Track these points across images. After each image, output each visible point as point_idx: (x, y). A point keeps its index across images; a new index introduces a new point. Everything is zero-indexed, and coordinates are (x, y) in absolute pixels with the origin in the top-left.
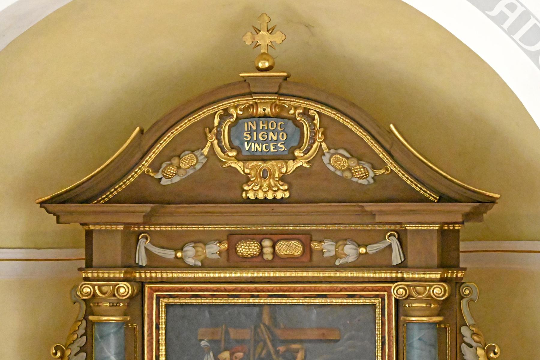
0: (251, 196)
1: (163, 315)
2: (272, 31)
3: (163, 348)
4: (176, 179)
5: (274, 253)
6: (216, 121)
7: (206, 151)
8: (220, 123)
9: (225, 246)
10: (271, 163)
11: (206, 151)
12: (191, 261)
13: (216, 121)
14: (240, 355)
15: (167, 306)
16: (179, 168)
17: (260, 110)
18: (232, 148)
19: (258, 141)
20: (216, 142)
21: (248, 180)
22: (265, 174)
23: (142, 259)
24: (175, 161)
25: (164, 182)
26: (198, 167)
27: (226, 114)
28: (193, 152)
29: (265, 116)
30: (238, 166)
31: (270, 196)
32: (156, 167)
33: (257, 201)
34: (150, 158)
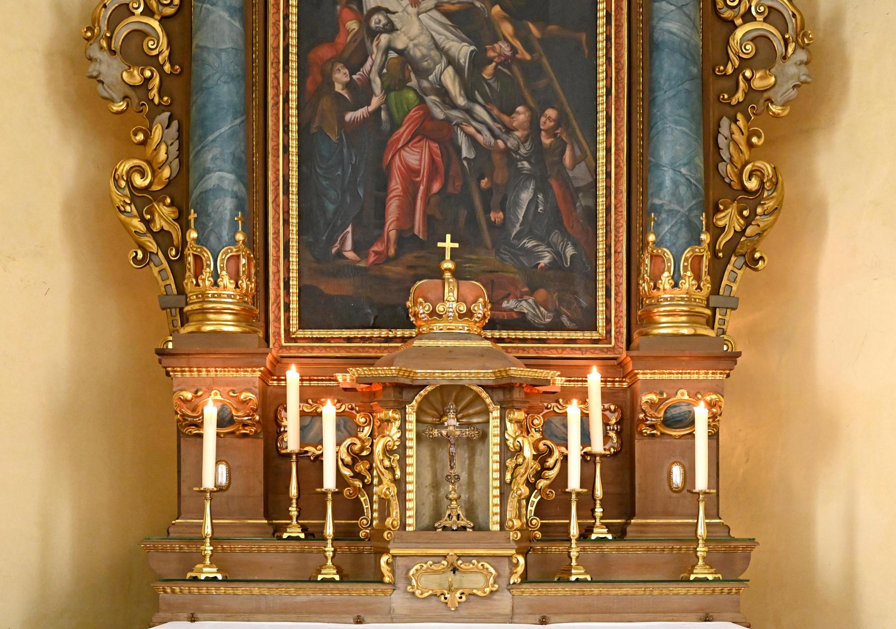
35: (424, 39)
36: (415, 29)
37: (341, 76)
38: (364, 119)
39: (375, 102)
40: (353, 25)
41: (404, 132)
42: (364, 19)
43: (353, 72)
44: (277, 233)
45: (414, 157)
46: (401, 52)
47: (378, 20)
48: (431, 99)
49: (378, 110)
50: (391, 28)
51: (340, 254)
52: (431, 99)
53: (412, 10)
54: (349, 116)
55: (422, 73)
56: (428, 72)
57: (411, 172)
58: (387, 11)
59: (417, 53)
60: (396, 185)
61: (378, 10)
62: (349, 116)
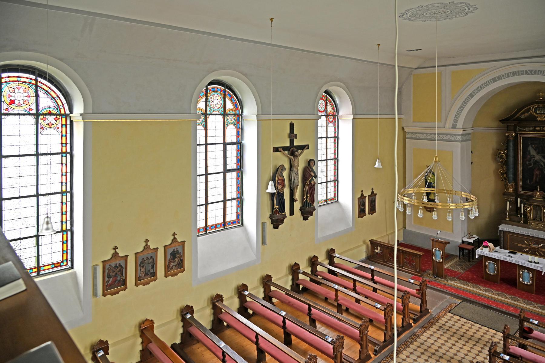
0: (538, 120)
1: (521, 139)
2: (542, 93)
3: (521, 144)
4: (524, 117)
5: (543, 129)
6: (532, 108)
7: (530, 113)
8: (532, 108)
9: (533, 128)
10: (542, 115)
11: (530, 113)
12: (527, 130)
13: (532, 108)
14: (536, 146)
15: (522, 137)
16: (524, 115)
17: (540, 106)
18: (535, 112)
19: (540, 111)
20: (531, 111)
21: (538, 117)
22: (541, 116)
23: (517, 129)
24: (524, 114)
25: (522, 117)
26: (528, 115)
27: (533, 107)
28: (527, 113)
29: (541, 107)
30: (536, 115)
31: (542, 120)
32: (520, 115)
33: (539, 121)
34: (519, 114)
35: (539, 159)
36: (537, 158)
37: (527, 163)
38: (530, 168)
39: (532, 166)
40: (529, 157)
41: (536, 169)
42: (531, 156)
43: (529, 162)
44: (519, 179)
45: (537, 172)
46: (536, 160)
47: (532, 156)
48: (540, 166)
49: (532, 167)
50: (534, 157)
51: (527, 183)
52: (540, 166)
53: (537, 155)
54: (529, 167)
55: (538, 163)
56: (539, 163)
57: (537, 175)
58: (534, 155)
59: (538, 160)
60: (535, 175)
61: (532, 155)
62: (529, 167)
